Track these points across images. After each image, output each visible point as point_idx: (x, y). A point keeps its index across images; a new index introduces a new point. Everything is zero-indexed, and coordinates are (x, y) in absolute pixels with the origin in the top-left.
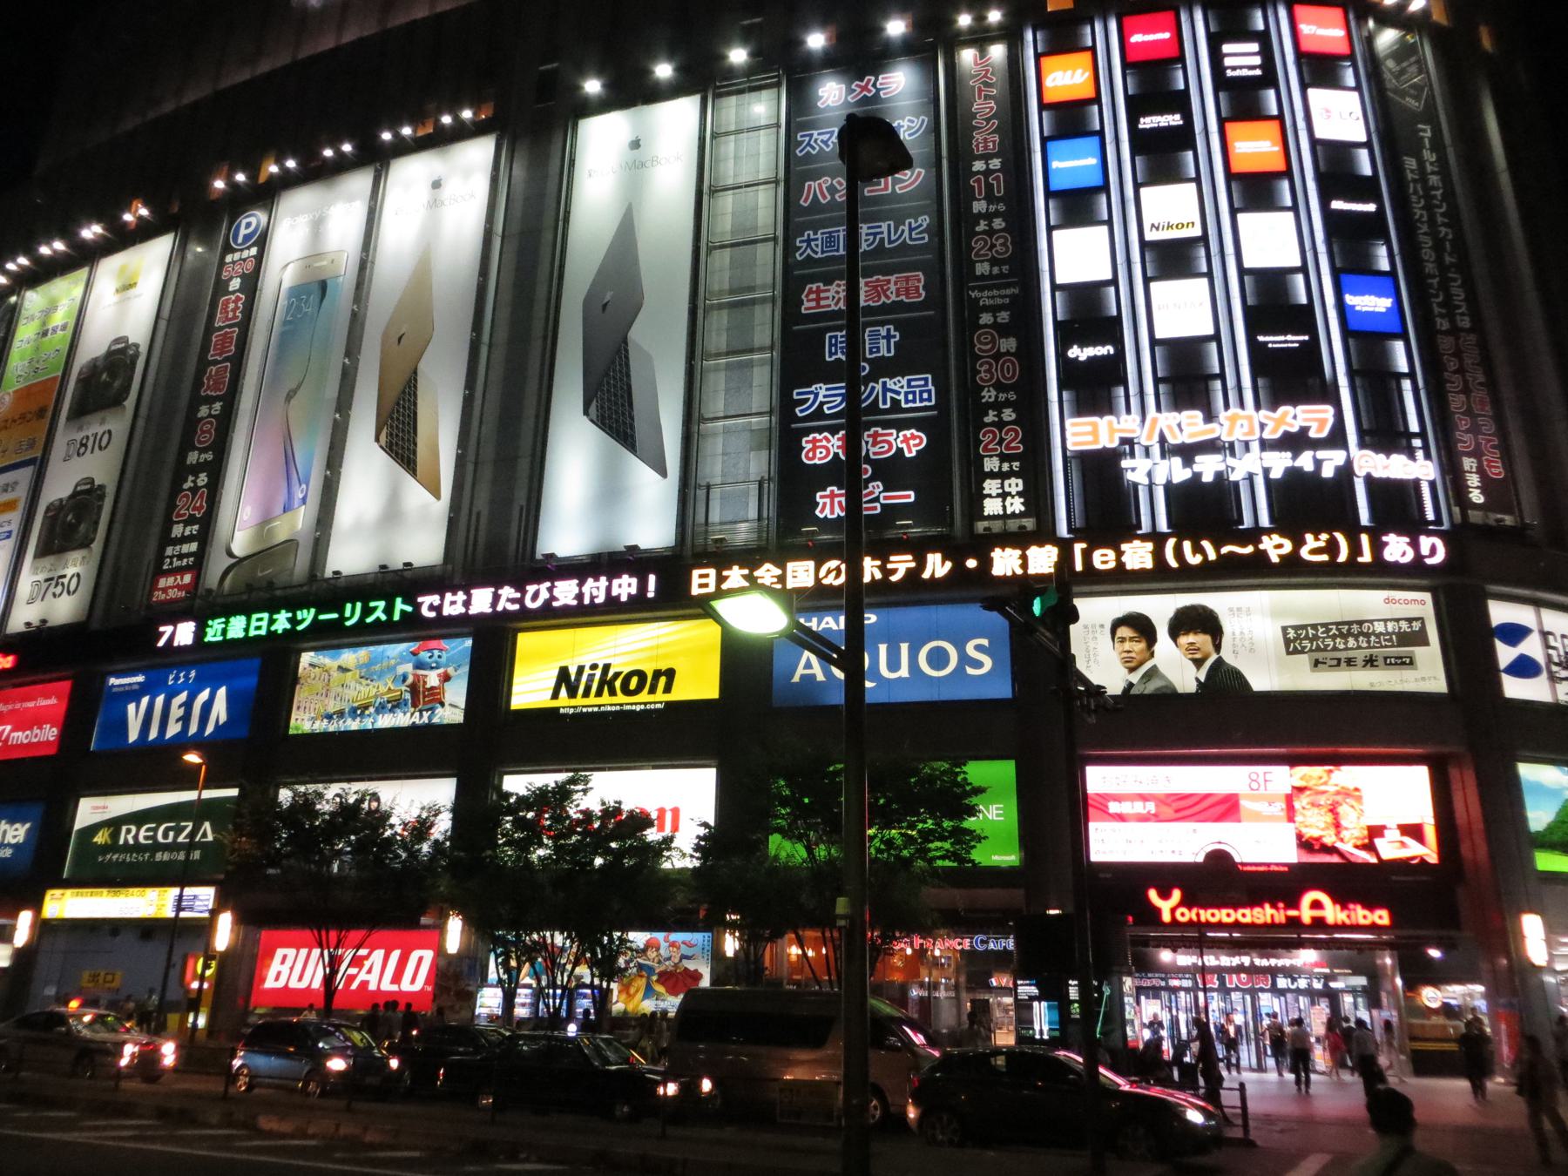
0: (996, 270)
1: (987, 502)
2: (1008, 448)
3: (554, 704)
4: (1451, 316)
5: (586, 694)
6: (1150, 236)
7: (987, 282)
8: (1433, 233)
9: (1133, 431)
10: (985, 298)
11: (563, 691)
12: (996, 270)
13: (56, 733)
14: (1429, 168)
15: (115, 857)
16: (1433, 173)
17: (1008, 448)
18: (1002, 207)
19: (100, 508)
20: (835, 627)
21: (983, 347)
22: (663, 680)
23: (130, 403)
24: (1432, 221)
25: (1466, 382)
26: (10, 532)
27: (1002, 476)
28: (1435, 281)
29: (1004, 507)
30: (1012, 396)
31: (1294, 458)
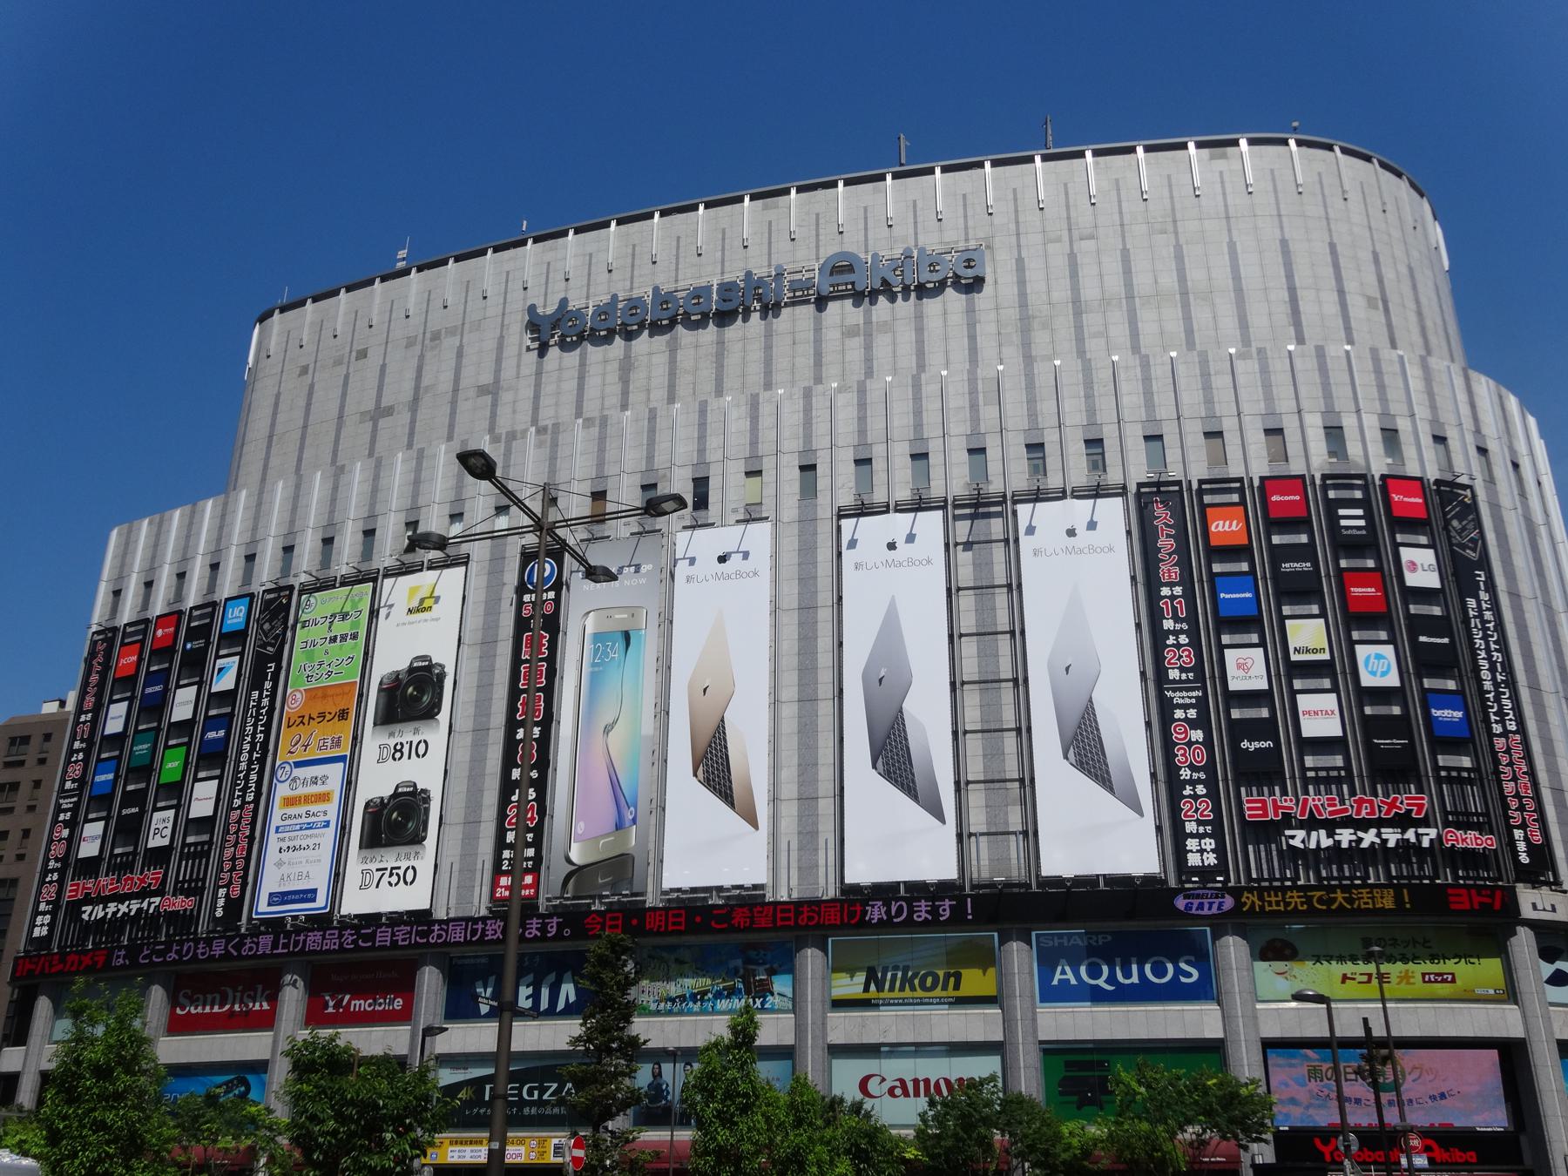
0: (1184, 676)
1: (1190, 856)
2: (1202, 815)
3: (866, 996)
4: (1502, 722)
5: (892, 989)
6: (1294, 657)
7: (1180, 686)
8: (1489, 658)
9: (1291, 808)
10: (1178, 697)
11: (873, 987)
12: (1184, 676)
13: (401, 1003)
14: (1484, 606)
15: (482, 1111)
16: (1488, 609)
17: (1202, 815)
18: (1185, 626)
19: (427, 811)
20: (1080, 943)
21: (1179, 736)
22: (952, 980)
23: (443, 716)
24: (1488, 650)
25: (1514, 771)
26: (328, 822)
27: (1200, 836)
28: (1491, 696)
29: (1203, 860)
30: (1203, 776)
31: (1403, 833)
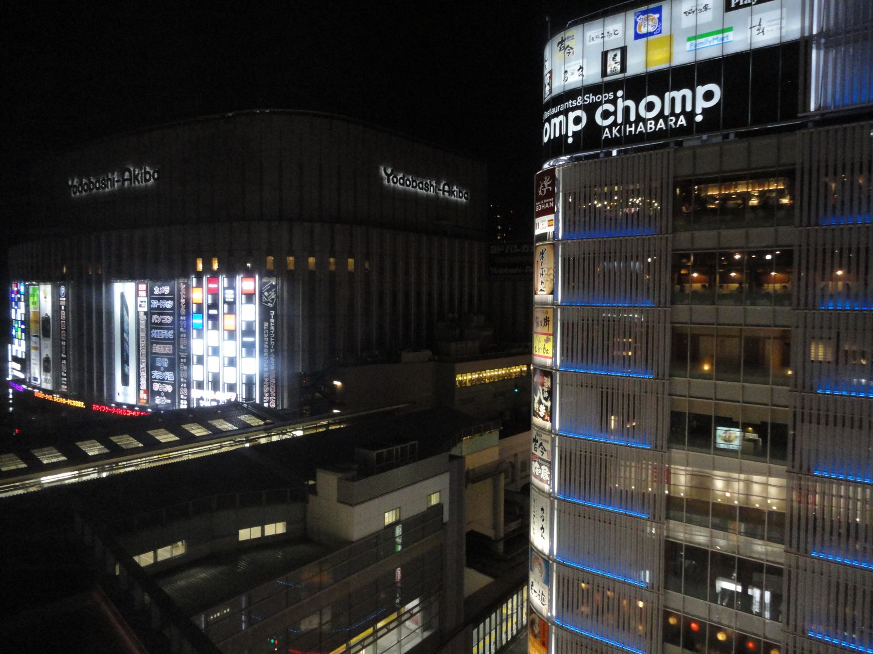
14: (271, 324)
24: (269, 342)
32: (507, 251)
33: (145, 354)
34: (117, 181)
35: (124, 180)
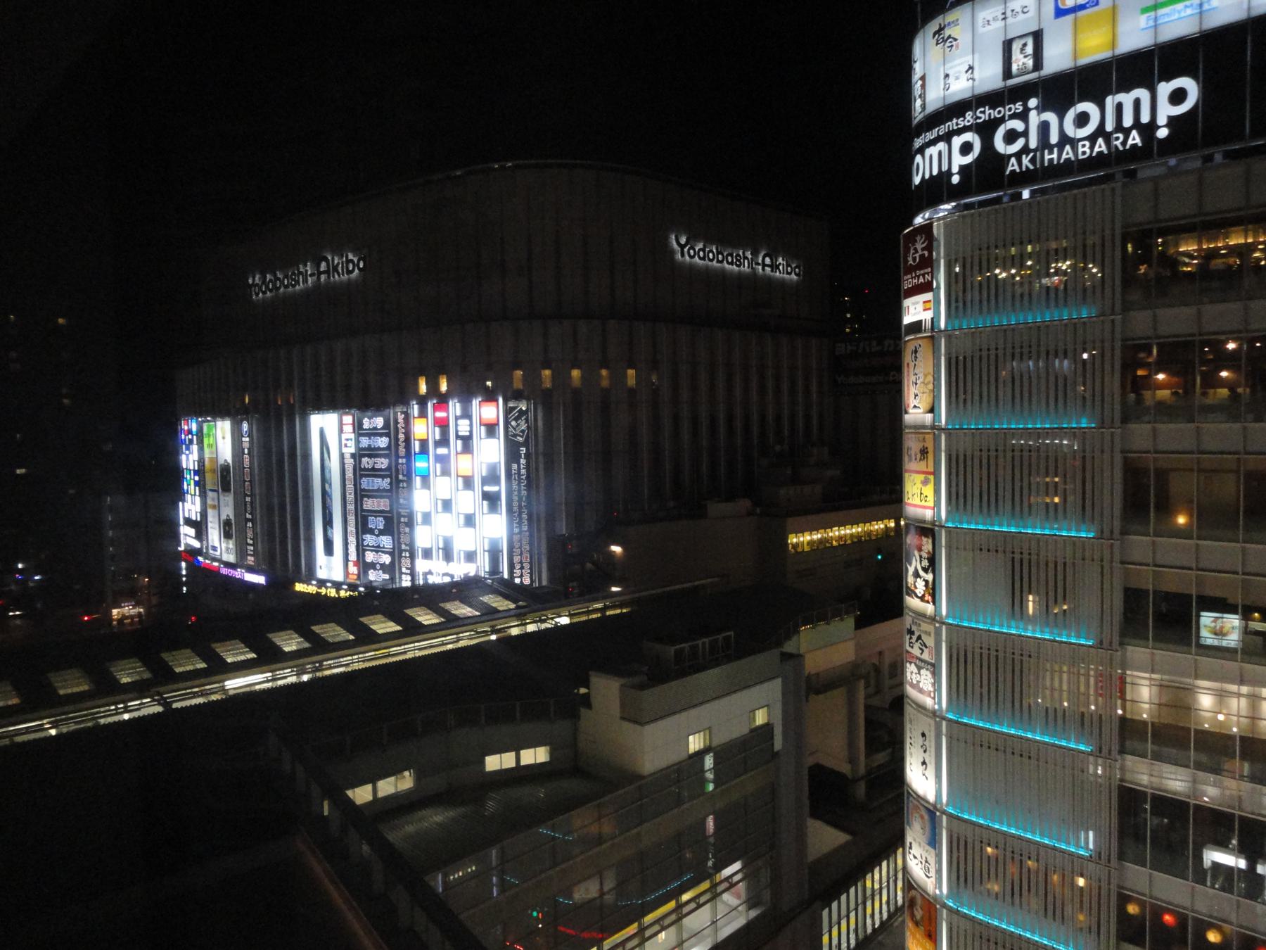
14: (522, 466)
24: (519, 491)
32: (860, 351)
33: (353, 512)
34: (312, 275)
35: (320, 273)
